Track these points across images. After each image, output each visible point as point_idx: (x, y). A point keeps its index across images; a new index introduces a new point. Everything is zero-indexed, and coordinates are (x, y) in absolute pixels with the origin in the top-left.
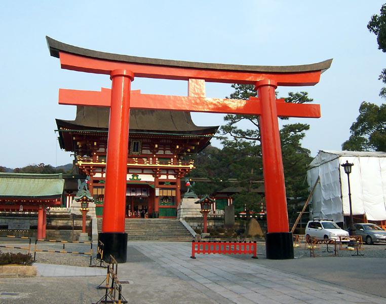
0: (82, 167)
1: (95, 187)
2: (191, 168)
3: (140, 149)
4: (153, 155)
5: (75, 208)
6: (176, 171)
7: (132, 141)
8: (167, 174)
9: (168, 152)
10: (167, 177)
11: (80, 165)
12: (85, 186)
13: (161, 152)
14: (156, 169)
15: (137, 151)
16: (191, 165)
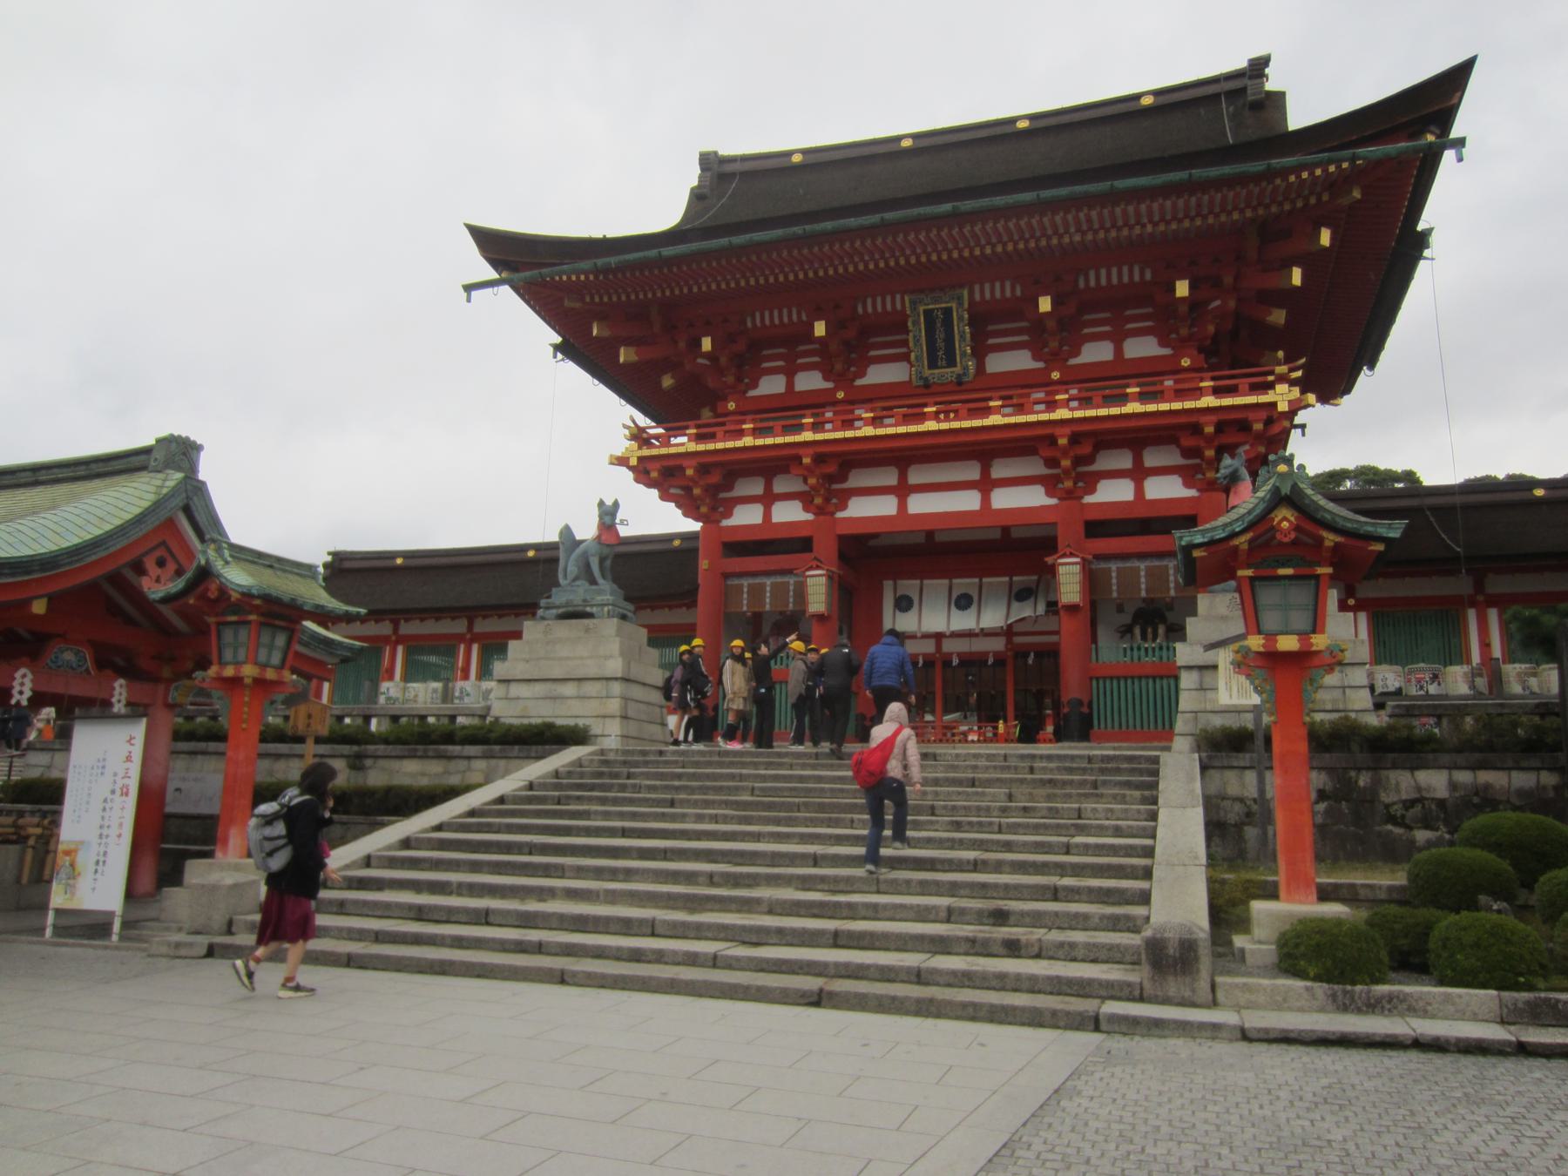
0: (647, 473)
1: (726, 576)
2: (1283, 407)
3: (962, 347)
4: (1048, 370)
5: (516, 690)
6: (1187, 442)
7: (914, 303)
8: (1139, 474)
9: (1142, 348)
10: (1139, 491)
11: (633, 462)
12: (588, 566)
13: (1097, 352)
14: (1052, 440)
15: (951, 362)
16: (1282, 388)
